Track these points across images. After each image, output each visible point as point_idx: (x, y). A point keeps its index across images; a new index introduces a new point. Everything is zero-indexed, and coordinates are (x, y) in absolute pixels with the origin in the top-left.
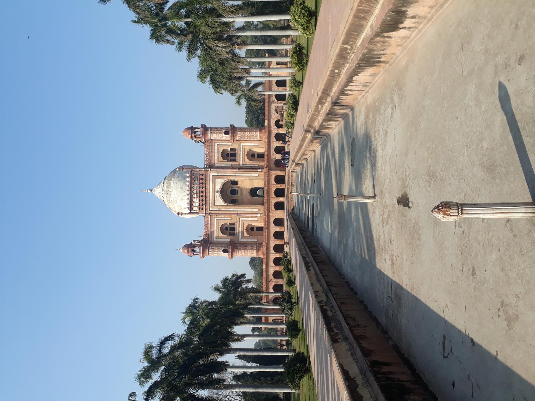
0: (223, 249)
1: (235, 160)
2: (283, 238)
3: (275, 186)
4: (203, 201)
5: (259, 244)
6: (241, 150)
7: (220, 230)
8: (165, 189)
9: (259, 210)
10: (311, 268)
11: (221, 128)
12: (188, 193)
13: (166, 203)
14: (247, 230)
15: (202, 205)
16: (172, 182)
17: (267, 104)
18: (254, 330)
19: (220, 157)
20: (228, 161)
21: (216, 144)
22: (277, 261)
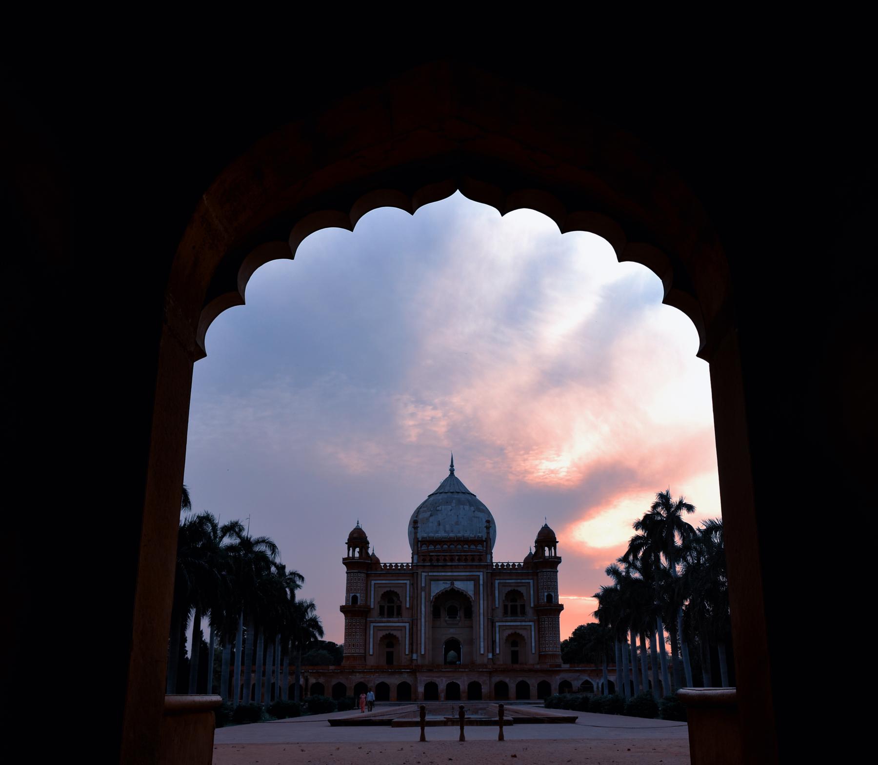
0: (358, 595)
1: (505, 613)
3: (463, 683)
4: (438, 560)
5: (365, 657)
6: (524, 624)
7: (388, 589)
8: (456, 496)
9: (423, 656)
11: (557, 589)
12: (452, 535)
13: (432, 499)
15: (431, 560)
16: (467, 507)
21: (531, 581)
22: (339, 689)
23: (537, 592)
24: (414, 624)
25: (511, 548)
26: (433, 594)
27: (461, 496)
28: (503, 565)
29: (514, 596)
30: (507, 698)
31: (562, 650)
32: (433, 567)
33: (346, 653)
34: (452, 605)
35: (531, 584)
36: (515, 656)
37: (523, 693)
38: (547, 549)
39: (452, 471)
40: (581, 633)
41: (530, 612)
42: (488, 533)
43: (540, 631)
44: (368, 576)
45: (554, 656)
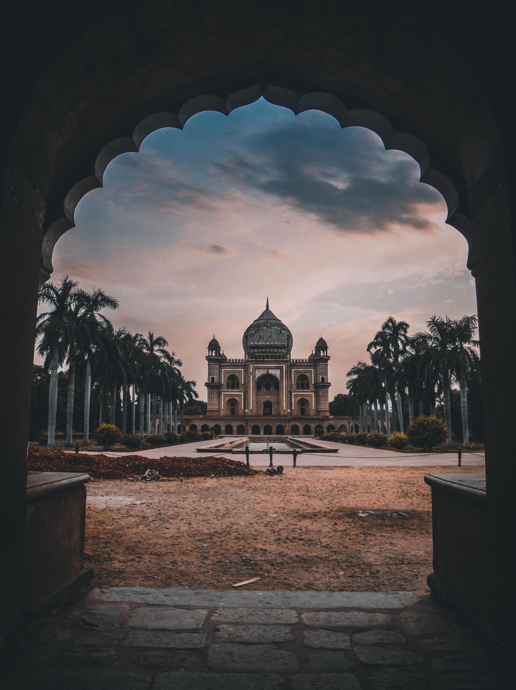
1: (298, 387)
5: (219, 411)
6: (308, 393)
7: (231, 374)
9: (251, 411)
10: (230, 445)
12: (268, 343)
15: (255, 358)
16: (276, 328)
17: (347, 417)
19: (300, 374)
20: (297, 381)
21: (313, 370)
24: (246, 393)
25: (301, 351)
26: (257, 377)
27: (273, 321)
28: (296, 361)
32: (257, 362)
33: (209, 408)
34: (267, 383)
35: (313, 372)
36: (303, 411)
37: (307, 431)
38: (322, 351)
39: (267, 306)
40: (339, 398)
41: (312, 387)
42: (288, 343)
44: (220, 366)
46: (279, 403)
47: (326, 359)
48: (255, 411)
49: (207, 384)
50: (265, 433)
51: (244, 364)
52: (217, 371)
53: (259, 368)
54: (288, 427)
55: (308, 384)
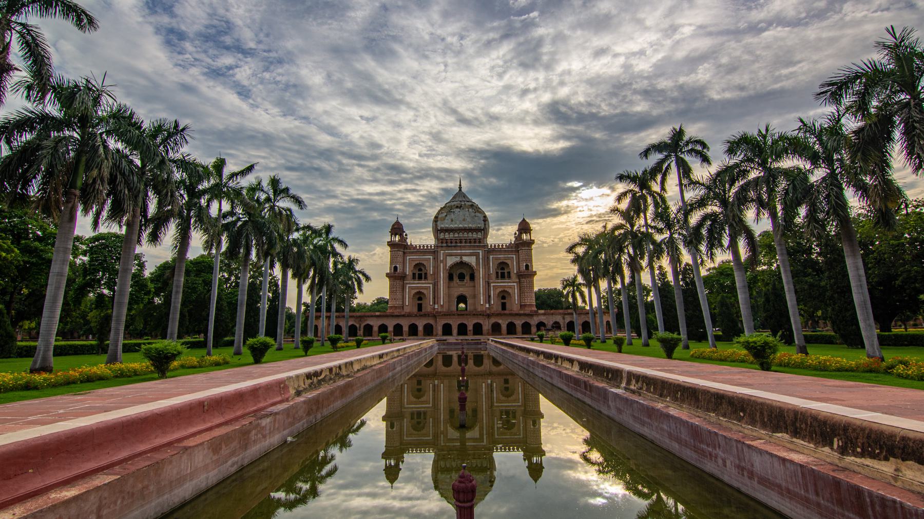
1: (497, 277)
2: (409, 335)
3: (470, 323)
9: (442, 306)
14: (419, 293)
17: (561, 311)
18: (305, 304)
23: (518, 263)
24: (436, 285)
29: (503, 265)
30: (501, 334)
31: (537, 299)
34: (461, 273)
36: (504, 306)
37: (511, 330)
41: (513, 276)
43: (520, 289)
44: (404, 253)
45: (531, 305)
46: (475, 296)
47: (531, 242)
48: (446, 307)
49: (388, 275)
50: (459, 334)
51: (434, 252)
52: (400, 259)
53: (451, 255)
54: (486, 325)
55: (509, 273)
